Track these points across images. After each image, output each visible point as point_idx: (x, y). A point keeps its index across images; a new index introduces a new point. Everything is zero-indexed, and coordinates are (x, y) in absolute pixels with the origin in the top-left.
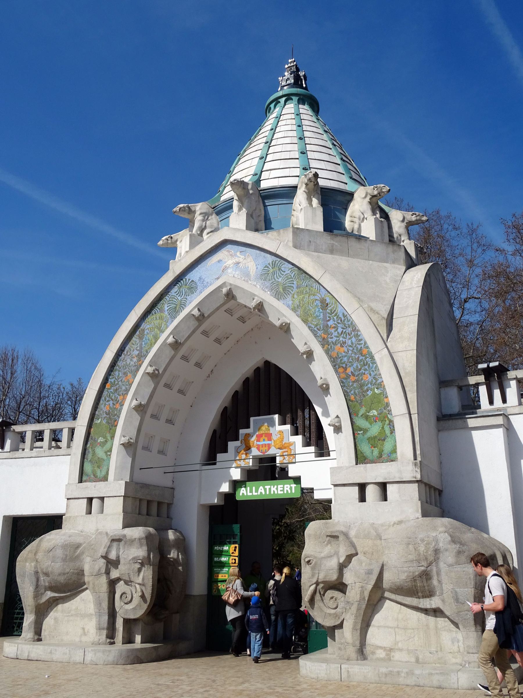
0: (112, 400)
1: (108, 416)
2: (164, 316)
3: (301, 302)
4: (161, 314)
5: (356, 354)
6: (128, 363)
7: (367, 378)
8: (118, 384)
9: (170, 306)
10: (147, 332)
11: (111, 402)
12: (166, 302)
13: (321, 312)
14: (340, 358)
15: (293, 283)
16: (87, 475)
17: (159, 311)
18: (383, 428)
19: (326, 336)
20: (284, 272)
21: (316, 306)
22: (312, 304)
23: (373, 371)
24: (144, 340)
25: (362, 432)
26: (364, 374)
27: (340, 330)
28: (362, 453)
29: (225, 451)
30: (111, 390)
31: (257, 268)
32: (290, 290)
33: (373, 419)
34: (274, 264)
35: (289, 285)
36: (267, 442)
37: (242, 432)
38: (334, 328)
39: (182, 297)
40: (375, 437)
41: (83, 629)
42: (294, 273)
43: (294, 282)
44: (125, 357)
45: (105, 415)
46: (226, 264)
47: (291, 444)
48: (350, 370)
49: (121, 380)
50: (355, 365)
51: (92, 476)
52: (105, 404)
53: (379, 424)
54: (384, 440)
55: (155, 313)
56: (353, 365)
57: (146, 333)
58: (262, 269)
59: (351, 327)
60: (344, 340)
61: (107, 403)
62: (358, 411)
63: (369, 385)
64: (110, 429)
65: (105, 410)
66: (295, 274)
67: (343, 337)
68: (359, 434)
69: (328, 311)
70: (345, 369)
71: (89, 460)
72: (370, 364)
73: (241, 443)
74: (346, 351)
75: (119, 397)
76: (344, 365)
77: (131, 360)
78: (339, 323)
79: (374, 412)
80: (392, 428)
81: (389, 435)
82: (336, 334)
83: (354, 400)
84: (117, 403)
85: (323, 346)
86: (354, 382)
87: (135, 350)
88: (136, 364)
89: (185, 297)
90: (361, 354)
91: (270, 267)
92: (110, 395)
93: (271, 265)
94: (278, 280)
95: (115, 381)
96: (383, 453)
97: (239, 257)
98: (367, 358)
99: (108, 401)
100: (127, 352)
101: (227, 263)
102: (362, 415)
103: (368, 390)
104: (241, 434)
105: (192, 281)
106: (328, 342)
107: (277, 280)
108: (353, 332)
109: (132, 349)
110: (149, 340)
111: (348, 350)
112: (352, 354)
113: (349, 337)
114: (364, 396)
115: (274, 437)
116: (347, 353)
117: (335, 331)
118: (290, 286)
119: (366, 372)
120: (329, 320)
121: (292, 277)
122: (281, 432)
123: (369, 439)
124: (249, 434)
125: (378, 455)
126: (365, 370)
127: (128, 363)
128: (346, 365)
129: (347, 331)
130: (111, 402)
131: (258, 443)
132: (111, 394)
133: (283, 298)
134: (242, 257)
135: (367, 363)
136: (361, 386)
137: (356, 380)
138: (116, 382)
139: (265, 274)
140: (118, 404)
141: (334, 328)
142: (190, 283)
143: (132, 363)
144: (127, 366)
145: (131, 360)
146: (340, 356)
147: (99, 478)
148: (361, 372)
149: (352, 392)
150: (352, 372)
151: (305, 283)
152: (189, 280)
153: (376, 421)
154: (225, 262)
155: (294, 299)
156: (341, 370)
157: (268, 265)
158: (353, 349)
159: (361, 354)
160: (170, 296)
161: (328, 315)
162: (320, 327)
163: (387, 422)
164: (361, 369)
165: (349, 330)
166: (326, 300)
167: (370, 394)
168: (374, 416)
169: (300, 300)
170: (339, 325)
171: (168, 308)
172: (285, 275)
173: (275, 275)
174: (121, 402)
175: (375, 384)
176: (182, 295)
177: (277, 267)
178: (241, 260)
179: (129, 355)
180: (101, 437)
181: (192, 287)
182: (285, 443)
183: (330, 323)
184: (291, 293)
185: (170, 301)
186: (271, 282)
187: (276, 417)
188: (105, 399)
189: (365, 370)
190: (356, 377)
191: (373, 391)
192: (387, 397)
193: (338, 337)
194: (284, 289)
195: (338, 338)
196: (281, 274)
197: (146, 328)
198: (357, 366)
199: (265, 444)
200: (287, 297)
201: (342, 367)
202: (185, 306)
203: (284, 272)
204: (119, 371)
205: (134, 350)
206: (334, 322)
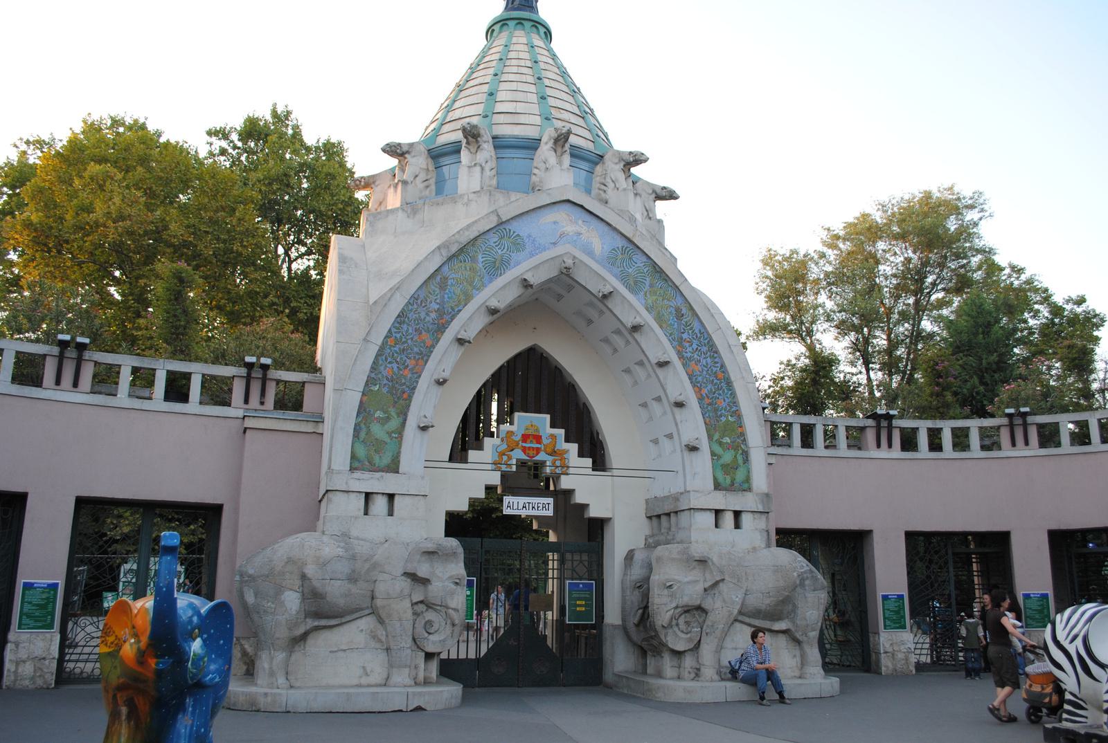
0: (397, 362)
4: (474, 265)
6: (422, 317)
7: (722, 404)
8: (404, 343)
16: (359, 461)
27: (695, 346)
29: (480, 447)
31: (603, 248)
34: (624, 251)
39: (504, 252)
40: (728, 464)
41: (364, 668)
45: (385, 382)
47: (567, 451)
48: (705, 391)
50: (709, 387)
51: (367, 463)
52: (386, 366)
53: (732, 452)
55: (465, 261)
57: (449, 283)
62: (713, 435)
63: (723, 411)
64: (396, 402)
65: (385, 373)
75: (408, 361)
76: (699, 385)
79: (727, 440)
85: (680, 358)
86: (708, 404)
92: (393, 355)
95: (401, 338)
98: (721, 383)
99: (390, 363)
105: (518, 235)
106: (683, 356)
115: (545, 441)
120: (683, 333)
122: (553, 437)
123: (722, 465)
126: (720, 394)
127: (422, 317)
130: (395, 366)
131: (524, 445)
134: (585, 228)
136: (716, 410)
138: (404, 340)
141: (688, 342)
145: (427, 314)
152: (514, 232)
154: (563, 227)
156: (698, 390)
159: (716, 377)
163: (740, 451)
165: (705, 349)
174: (411, 370)
178: (583, 231)
181: (518, 244)
183: (685, 336)
186: (620, 269)
187: (548, 417)
188: (386, 359)
189: (720, 394)
192: (741, 427)
194: (636, 283)
198: (711, 389)
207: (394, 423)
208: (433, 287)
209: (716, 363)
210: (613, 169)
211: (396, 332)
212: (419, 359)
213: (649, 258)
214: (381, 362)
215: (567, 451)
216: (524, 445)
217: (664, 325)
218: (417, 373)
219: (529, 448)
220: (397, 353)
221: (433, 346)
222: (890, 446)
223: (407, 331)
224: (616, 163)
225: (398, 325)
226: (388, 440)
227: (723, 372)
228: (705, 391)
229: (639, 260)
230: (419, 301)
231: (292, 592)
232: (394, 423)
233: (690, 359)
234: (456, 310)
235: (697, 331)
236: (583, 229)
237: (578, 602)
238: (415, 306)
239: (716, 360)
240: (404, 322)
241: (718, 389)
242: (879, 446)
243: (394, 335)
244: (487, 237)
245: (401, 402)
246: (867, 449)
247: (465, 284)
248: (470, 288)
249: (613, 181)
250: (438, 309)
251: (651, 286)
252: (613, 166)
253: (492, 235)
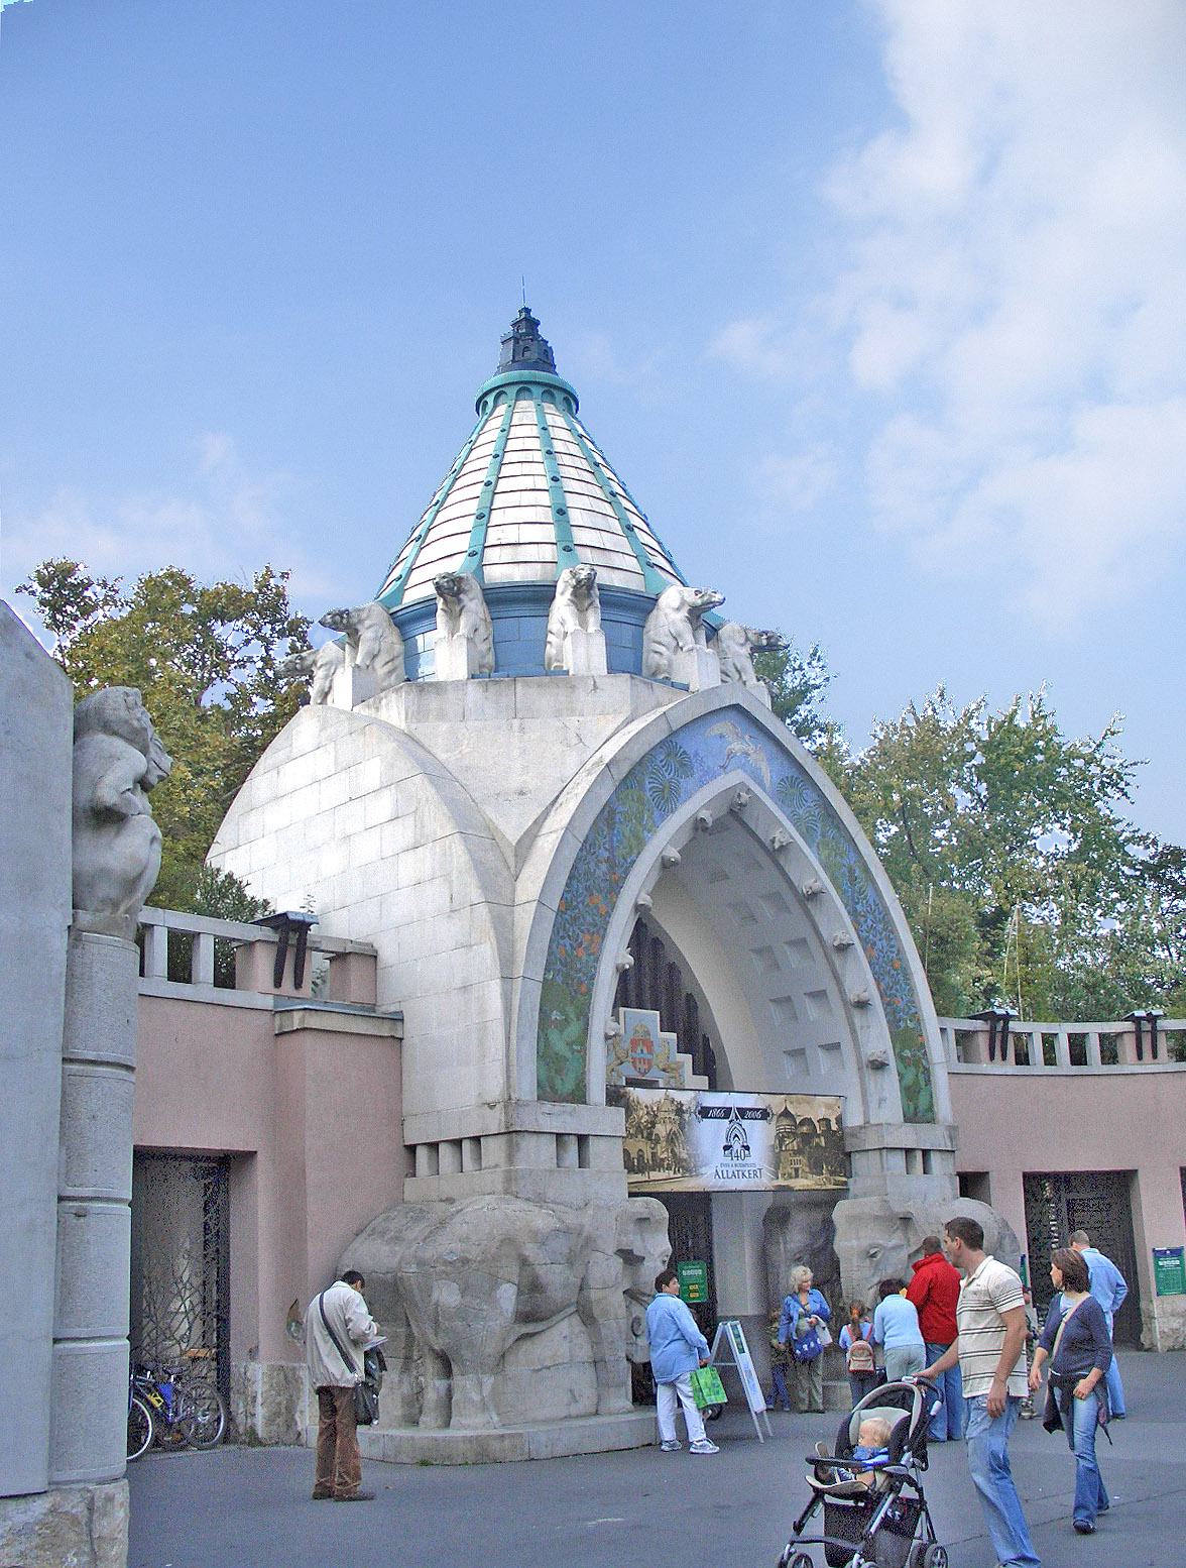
8: (576, 907)
27: (869, 922)
57: (618, 816)
64: (573, 998)
98: (898, 974)
99: (563, 938)
132: (567, 926)
207: (574, 1029)
209: (892, 947)
212: (593, 933)
218: (593, 954)
222: (1004, 1057)
224: (742, 645)
226: (568, 1055)
227: (900, 959)
231: (508, 1285)
232: (574, 1029)
235: (871, 902)
237: (691, 1287)
242: (992, 1057)
246: (979, 1062)
249: (738, 671)
251: (823, 835)
252: (737, 648)
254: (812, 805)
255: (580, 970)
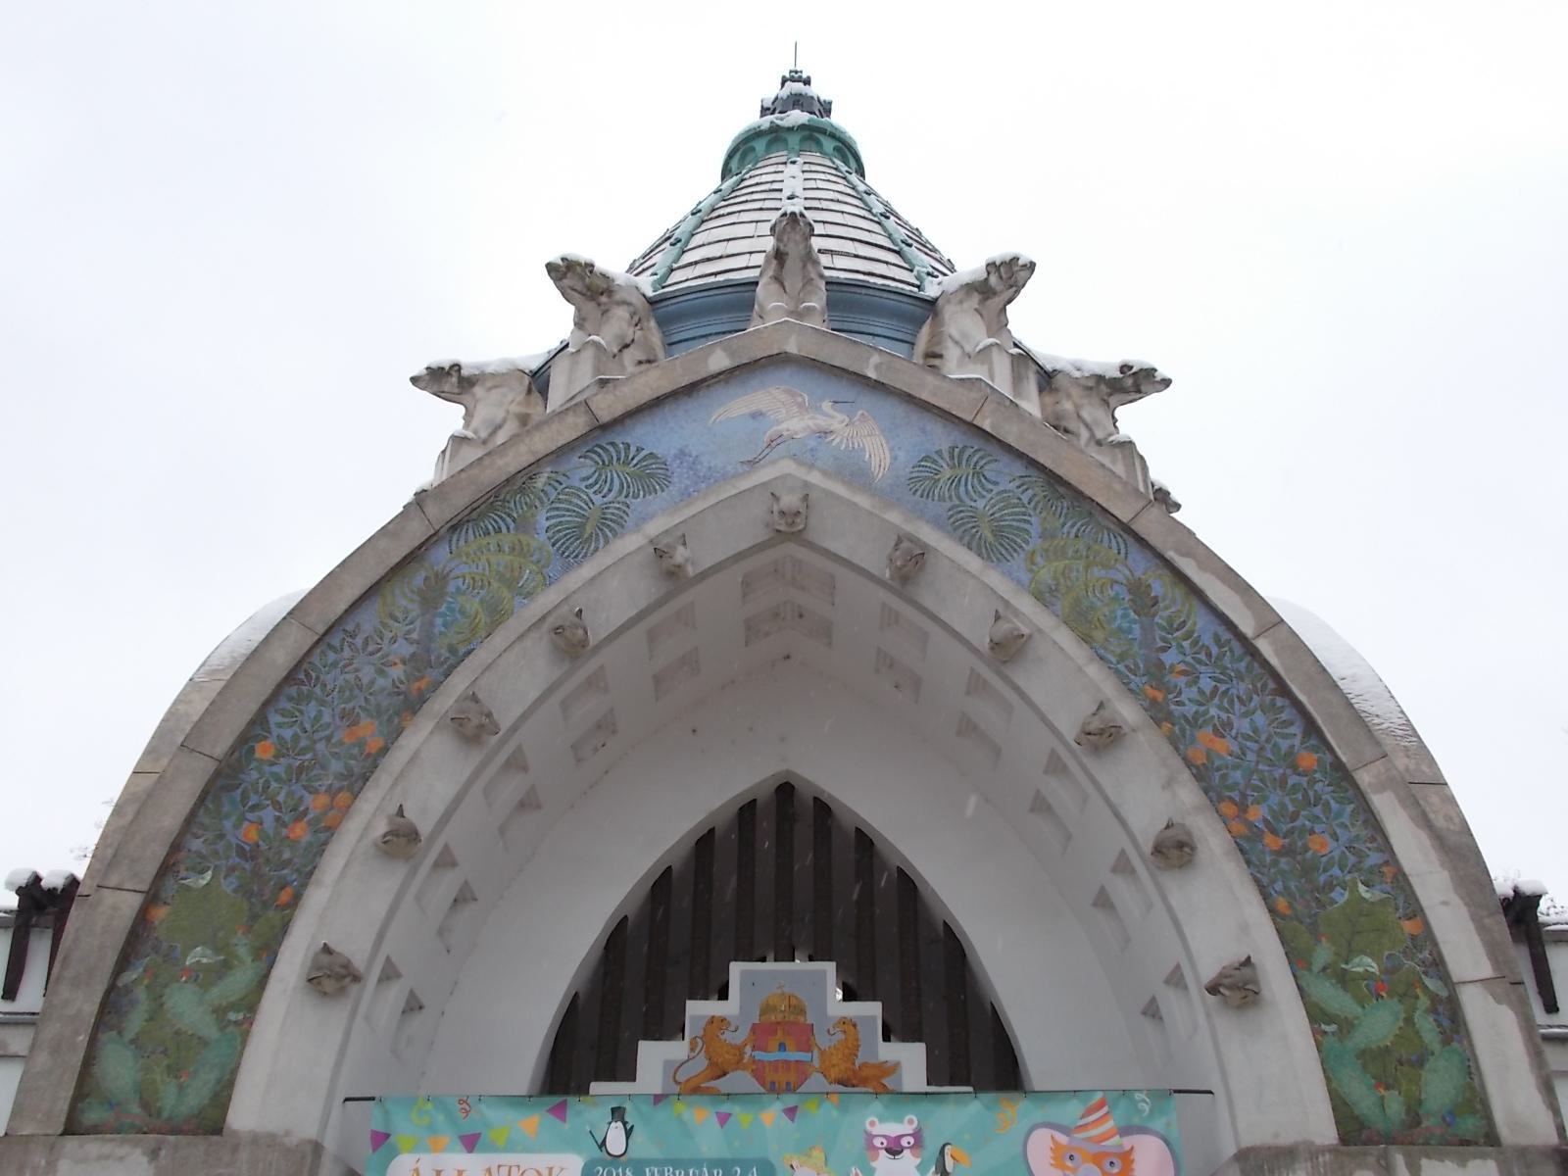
0: (277, 805)
1: (248, 866)
2: (534, 544)
3: (1062, 581)
4: (524, 538)
5: (1271, 763)
6: (365, 681)
8: (303, 751)
9: (558, 516)
10: (458, 589)
11: (269, 815)
12: (542, 502)
13: (1135, 622)
14: (1218, 769)
15: (1029, 522)
17: (512, 526)
18: (1409, 1021)
19: (1160, 696)
20: (996, 483)
21: (1116, 599)
22: (1102, 592)
23: (1343, 826)
24: (443, 609)
25: (1332, 1028)
26: (1312, 832)
27: (1206, 684)
28: (1346, 1103)
30: (275, 769)
31: (895, 458)
32: (1019, 541)
33: (1367, 986)
34: (956, 456)
35: (1015, 523)
36: (793, 1055)
37: (698, 1010)
38: (1183, 673)
40: (1385, 1051)
42: (1030, 492)
43: (1033, 519)
44: (353, 658)
46: (779, 428)
47: (893, 1068)
48: (1257, 813)
49: (328, 739)
50: (1275, 798)
51: (135, 1109)
53: (1394, 1005)
54: (1420, 1063)
55: (498, 531)
56: (1265, 799)
57: (451, 588)
58: (915, 462)
59: (1247, 680)
60: (1224, 716)
61: (249, 816)
63: (1336, 871)
64: (254, 917)
66: (1035, 495)
67: (1221, 708)
68: (1325, 1032)
69: (1157, 619)
70: (1242, 807)
71: (129, 1035)
72: (1332, 802)
73: (692, 1050)
74: (1236, 749)
75: (309, 799)
76: (1235, 795)
77: (381, 672)
78: (1200, 662)
79: (1366, 964)
80: (1446, 1023)
81: (1436, 1047)
82: (1192, 693)
83: (1288, 912)
84: (297, 819)
86: (1282, 852)
87: (401, 640)
88: (403, 687)
89: (622, 498)
90: (1294, 768)
91: (941, 462)
92: (267, 786)
93: (946, 456)
94: (973, 504)
95: (296, 738)
96: (1421, 1112)
97: (827, 415)
98: (1313, 782)
100: (366, 642)
101: (783, 426)
102: (1324, 969)
103: (1330, 886)
104: (693, 1018)
106: (1170, 713)
107: (969, 503)
108: (1255, 696)
109: (388, 635)
110: (462, 612)
111: (1241, 749)
112: (1258, 763)
113: (1244, 709)
114: (1321, 905)
115: (822, 1040)
116: (1238, 757)
117: (1189, 685)
118: (1018, 528)
119: (1318, 828)
120: (1164, 650)
121: (1026, 501)
122: (848, 1024)
124: (723, 1020)
125: (1403, 1116)
126: (1315, 819)
127: (365, 681)
128: (1244, 796)
129: (1234, 691)
131: (759, 1055)
132: (274, 785)
133: (998, 559)
134: (840, 416)
135: (1318, 798)
137: (1283, 846)
138: (304, 743)
139: (926, 478)
140: (303, 824)
141: (1183, 673)
142: (644, 458)
143: (381, 682)
144: (361, 689)
146: (1217, 763)
147: (170, 1118)
148: (1297, 823)
149: (1279, 886)
150: (1265, 820)
151: (1073, 526)
152: (641, 449)
153: (1379, 996)
154: (778, 422)
155: (1034, 567)
156: (1228, 809)
157: (936, 457)
158: (1262, 748)
159: (1294, 768)
160: (560, 488)
161: (1159, 633)
162: (1136, 665)
163: (1424, 1002)
164: (1294, 817)
165: (1242, 688)
166: (1149, 586)
167: (1341, 901)
168: (1367, 976)
169: (1055, 572)
170: (1202, 669)
171: (548, 524)
172: (999, 493)
173: (962, 489)
174: (317, 820)
175: (1356, 868)
176: (610, 490)
177: (968, 465)
179: (372, 654)
180: (204, 944)
182: (864, 1065)
183: (1170, 658)
184: (1021, 547)
185: (560, 501)
186: (948, 504)
188: (245, 797)
189: (1315, 819)
190: (1284, 838)
191: (1351, 892)
193: (1202, 704)
194: (998, 533)
195: (1202, 708)
196: (983, 488)
197: (457, 572)
198: (1283, 806)
199: (787, 1062)
200: (1009, 558)
201: (1231, 799)
202: (623, 527)
203: (996, 483)
204: (322, 703)
205: (394, 640)
206: (1181, 657)
207: (238, 981)
208: (404, 602)
210: (964, 325)
211: (280, 725)
212: (341, 789)
213: (1033, 463)
214: (226, 808)
215: (893, 1068)
216: (759, 1055)
217: (1099, 635)
219: (775, 1065)
220: (278, 779)
221: (384, 750)
223: (317, 718)
225: (289, 706)
226: (211, 1031)
228: (1257, 813)
229: (1005, 474)
230: (359, 641)
232: (238, 981)
233: (1195, 722)
234: (462, 650)
236: (835, 420)
238: (347, 653)
239: (1284, 716)
240: (309, 697)
241: (1308, 803)
243: (275, 731)
244: (561, 469)
245: (271, 913)
247: (495, 585)
248: (506, 594)
250: (413, 655)
253: (575, 460)
254: (1012, 486)
255: (289, 861)
